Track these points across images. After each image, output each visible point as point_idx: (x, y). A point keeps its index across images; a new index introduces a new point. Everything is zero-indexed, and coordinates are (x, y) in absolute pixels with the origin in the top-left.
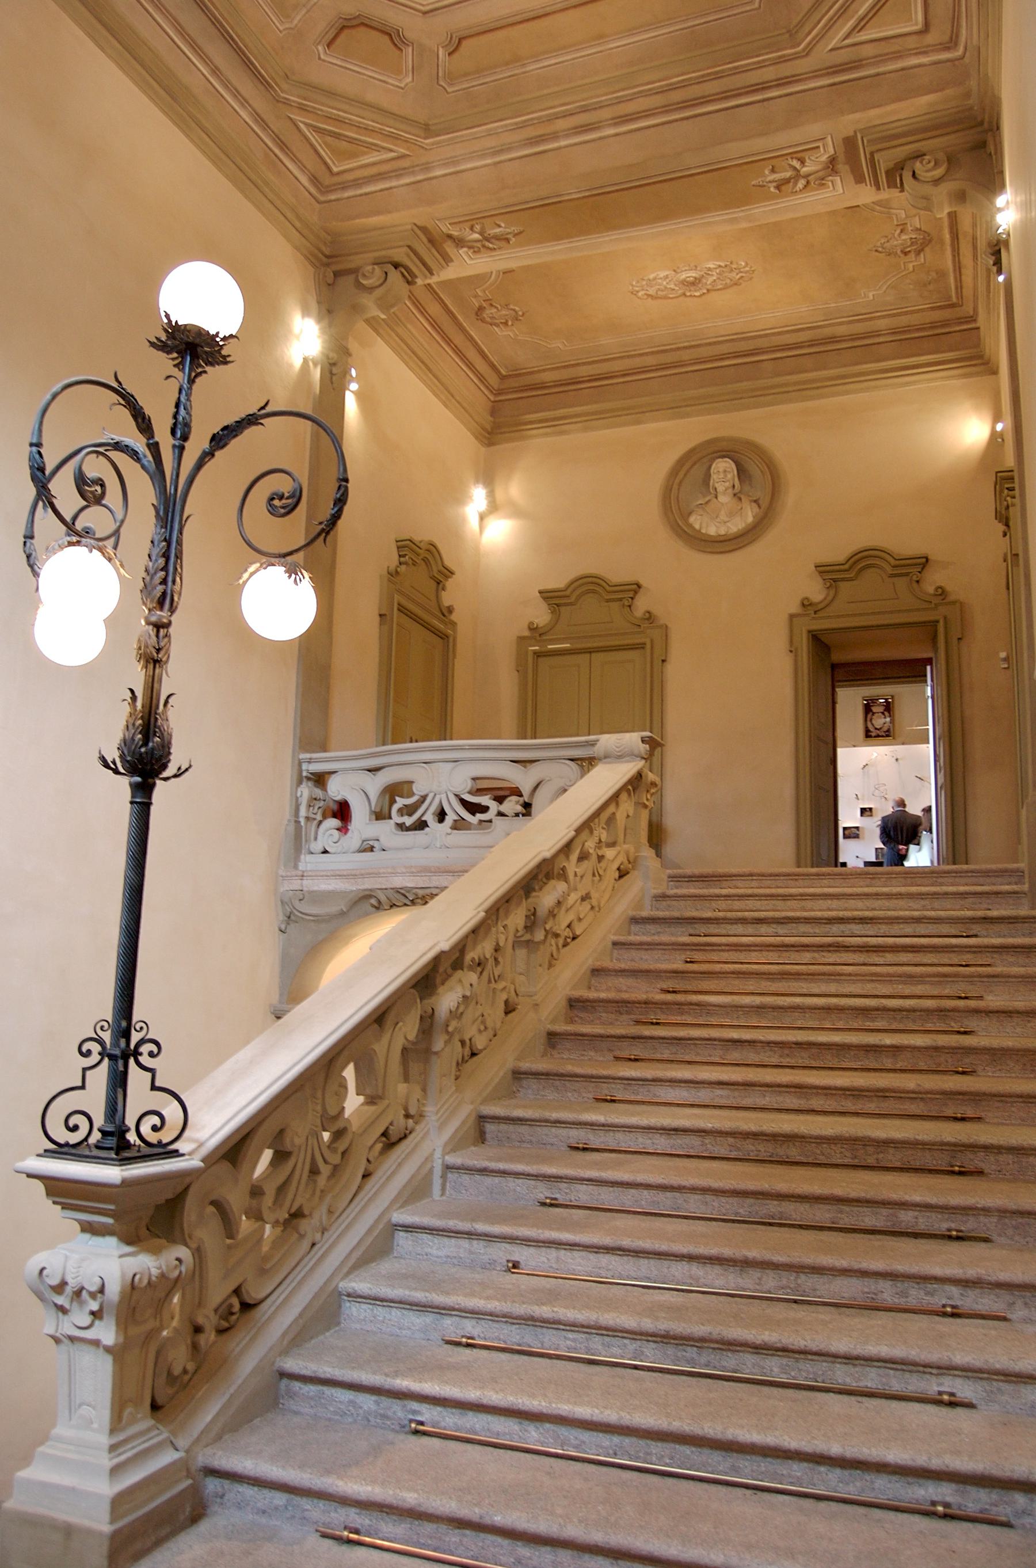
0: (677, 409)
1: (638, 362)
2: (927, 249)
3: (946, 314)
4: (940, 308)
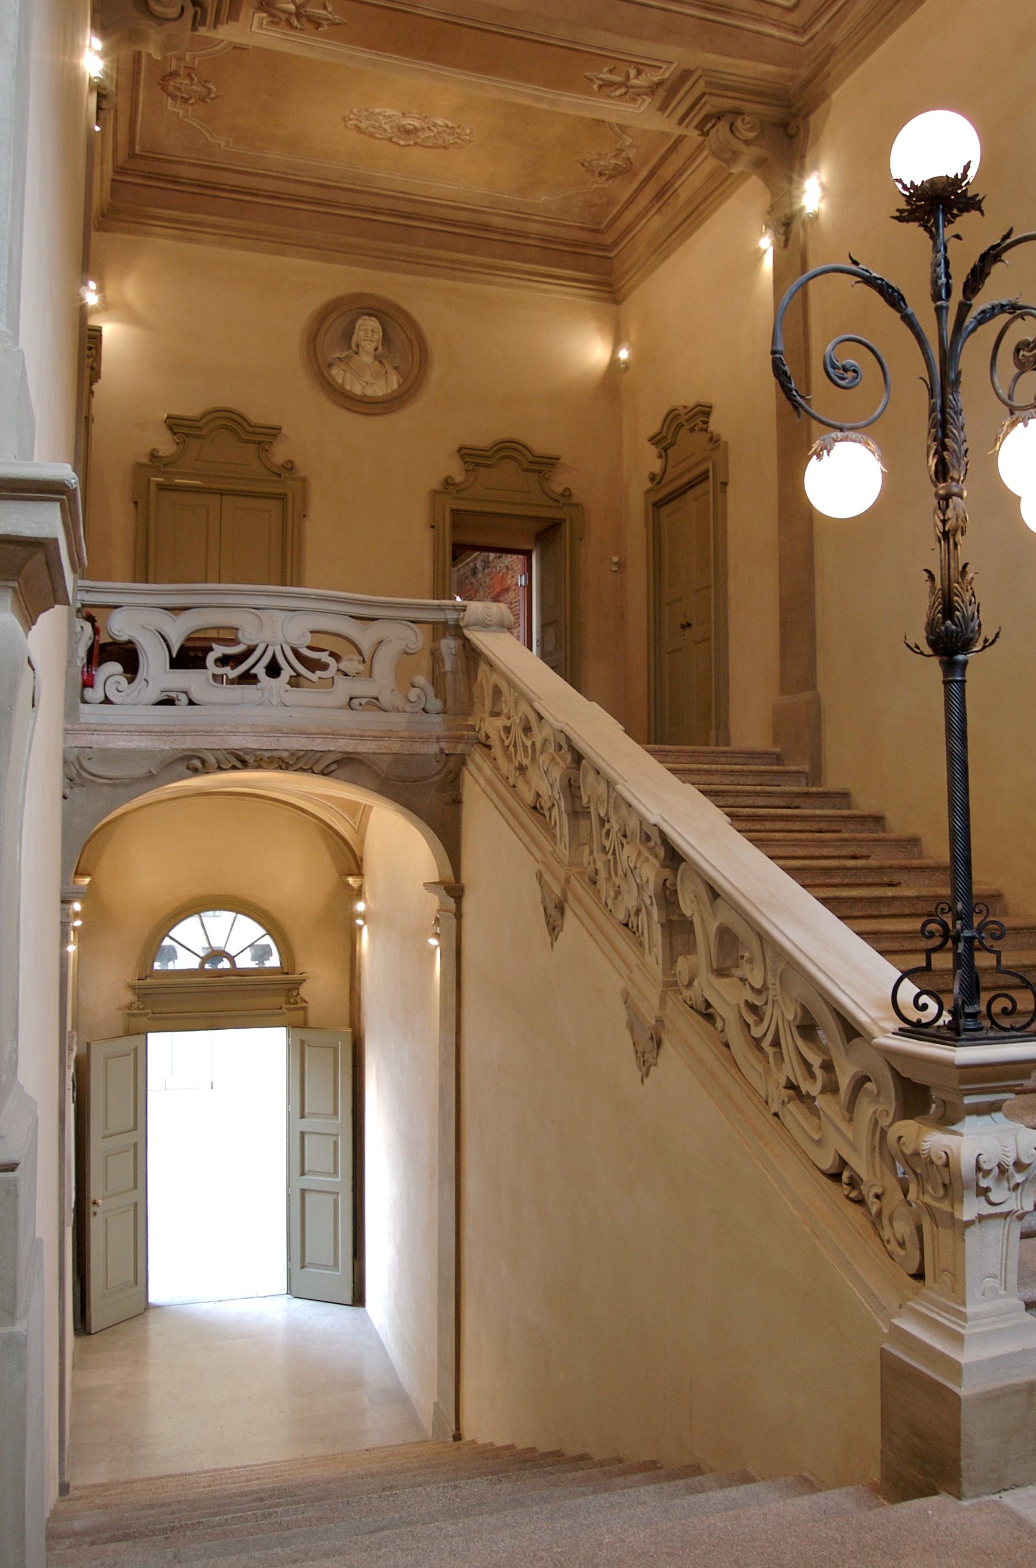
0: (327, 252)
1: (291, 188)
2: (619, 178)
3: (589, 237)
4: (588, 230)
